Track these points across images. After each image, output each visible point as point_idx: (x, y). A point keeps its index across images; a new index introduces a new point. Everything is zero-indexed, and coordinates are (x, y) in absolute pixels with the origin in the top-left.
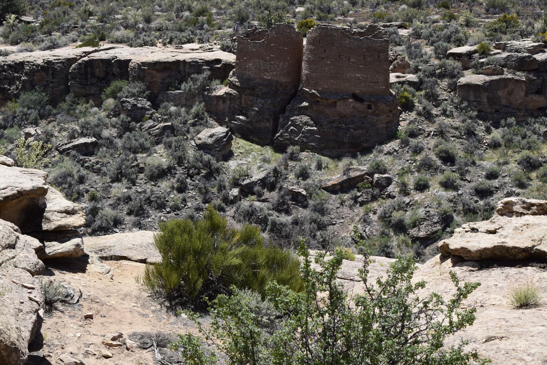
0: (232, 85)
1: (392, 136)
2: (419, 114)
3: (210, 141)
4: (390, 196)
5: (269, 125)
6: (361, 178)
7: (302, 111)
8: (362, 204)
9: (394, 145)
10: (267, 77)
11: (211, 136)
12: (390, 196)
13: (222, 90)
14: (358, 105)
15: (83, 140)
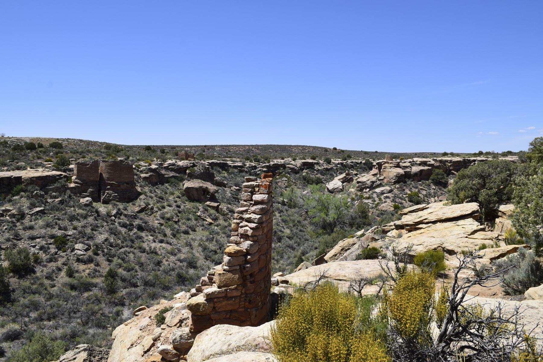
0: (75, 183)
1: (140, 194)
2: (140, 187)
3: (87, 203)
4: (157, 212)
5: (97, 195)
6: (145, 207)
7: (108, 189)
8: (150, 215)
9: (142, 197)
10: (92, 179)
11: (87, 201)
12: (157, 212)
13: (72, 185)
14: (128, 186)
15: (38, 209)
